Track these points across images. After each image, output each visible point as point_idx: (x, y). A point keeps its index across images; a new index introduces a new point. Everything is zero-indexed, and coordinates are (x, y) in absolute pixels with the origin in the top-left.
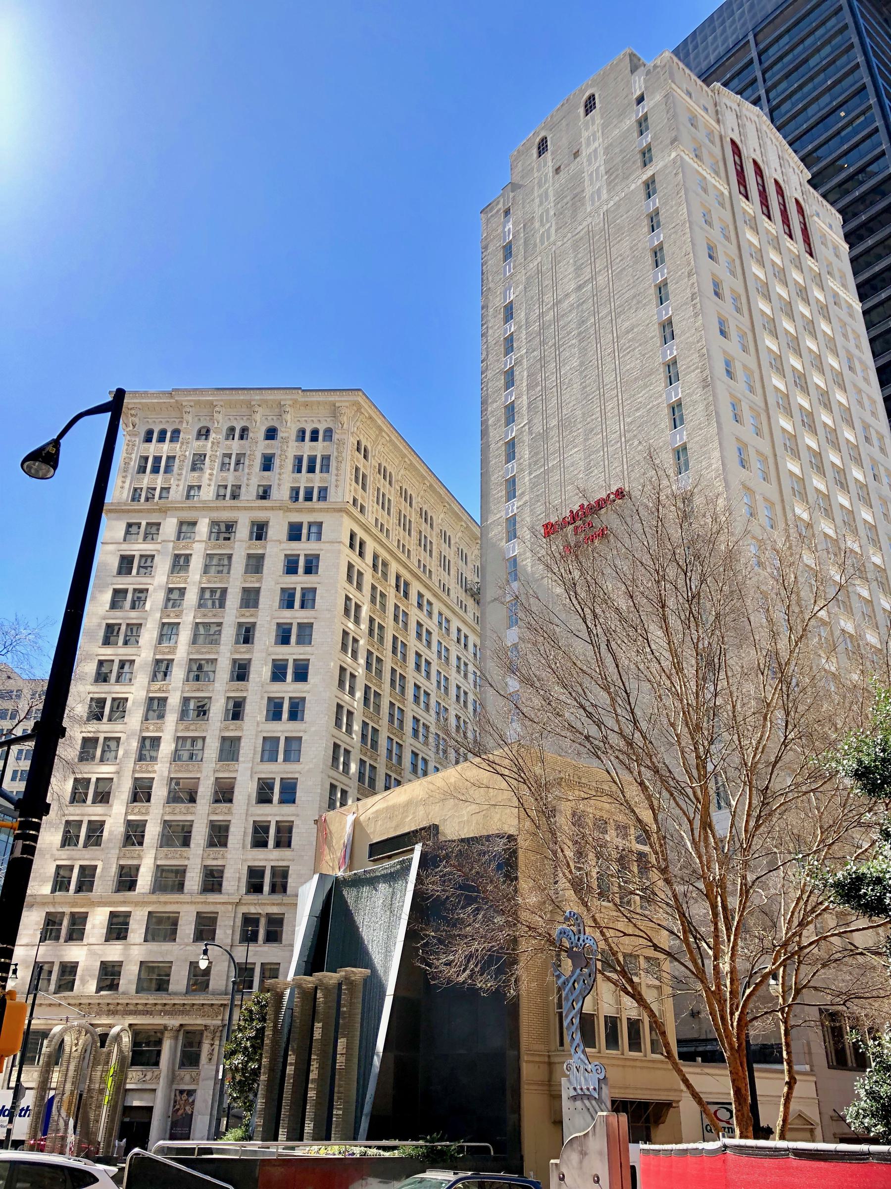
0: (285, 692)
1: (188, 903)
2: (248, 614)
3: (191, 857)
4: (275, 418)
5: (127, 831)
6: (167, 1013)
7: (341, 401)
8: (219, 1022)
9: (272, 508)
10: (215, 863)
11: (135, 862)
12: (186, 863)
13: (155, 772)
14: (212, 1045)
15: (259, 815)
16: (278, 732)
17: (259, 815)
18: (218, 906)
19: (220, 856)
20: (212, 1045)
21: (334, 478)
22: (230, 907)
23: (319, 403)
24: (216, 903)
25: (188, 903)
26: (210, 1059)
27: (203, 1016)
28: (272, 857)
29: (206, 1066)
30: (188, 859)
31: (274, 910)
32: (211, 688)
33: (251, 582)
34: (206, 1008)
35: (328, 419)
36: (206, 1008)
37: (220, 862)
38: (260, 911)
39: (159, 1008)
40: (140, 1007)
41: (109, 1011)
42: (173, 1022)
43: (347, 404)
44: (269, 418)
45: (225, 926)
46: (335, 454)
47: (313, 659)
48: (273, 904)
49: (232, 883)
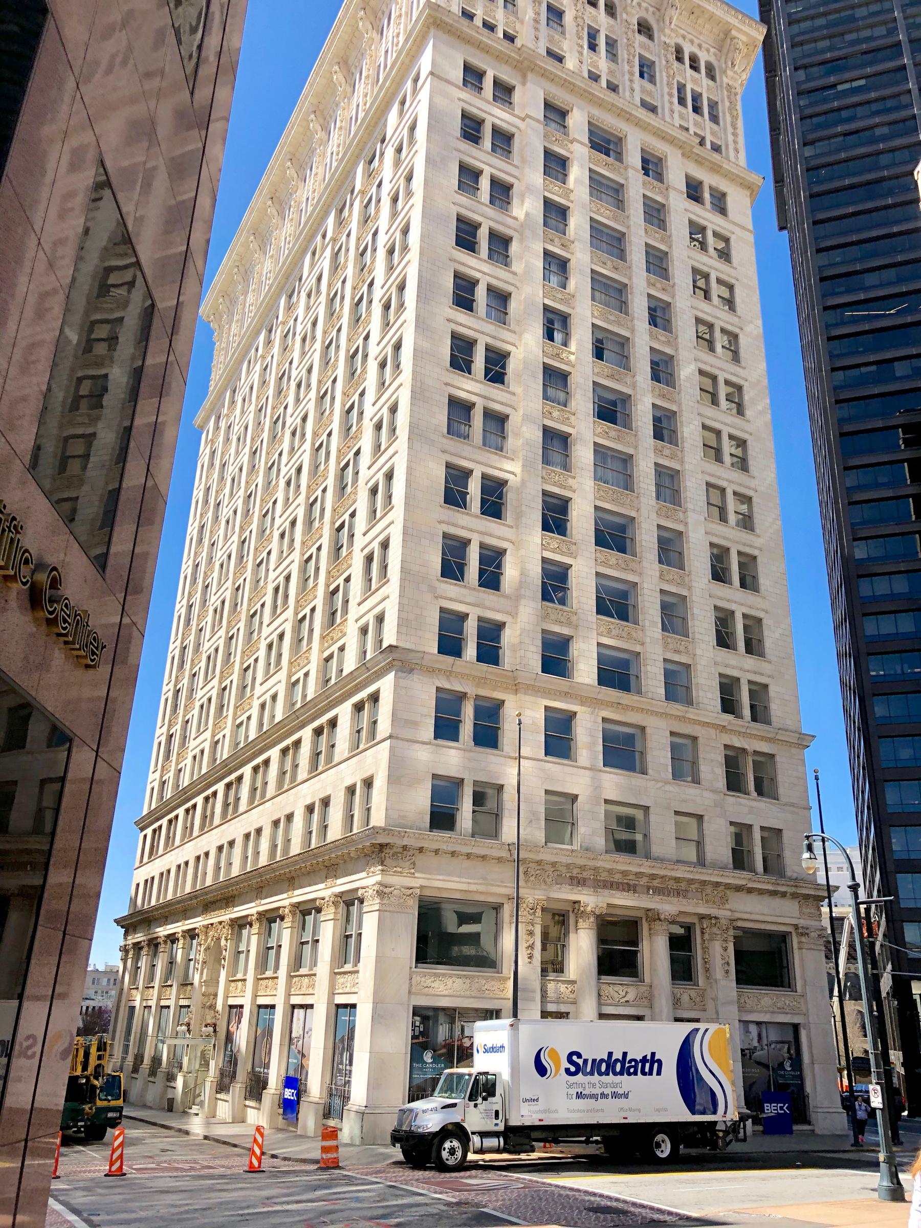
0: (726, 424)
1: (656, 713)
2: (659, 285)
3: (648, 640)
4: (651, 9)
5: (543, 578)
6: (659, 891)
7: (739, 30)
8: (728, 913)
9: (671, 140)
10: (676, 658)
11: (565, 631)
12: (638, 649)
13: (570, 488)
14: (725, 949)
15: (721, 599)
16: (723, 479)
17: (721, 599)
18: (697, 727)
19: (682, 648)
20: (725, 949)
21: (730, 138)
22: (712, 732)
23: (712, 16)
24: (695, 722)
25: (656, 713)
26: (727, 972)
27: (707, 902)
28: (746, 667)
29: (723, 983)
30: (643, 644)
31: (764, 747)
32: (629, 380)
33: (655, 239)
34: (709, 889)
35: (712, 50)
36: (709, 889)
37: (684, 659)
38: (746, 747)
39: (643, 881)
40: (617, 877)
41: (572, 878)
42: (668, 907)
43: (744, 38)
44: (644, 5)
45: (712, 761)
46: (727, 104)
47: (746, 386)
48: (762, 738)
49: (710, 695)
